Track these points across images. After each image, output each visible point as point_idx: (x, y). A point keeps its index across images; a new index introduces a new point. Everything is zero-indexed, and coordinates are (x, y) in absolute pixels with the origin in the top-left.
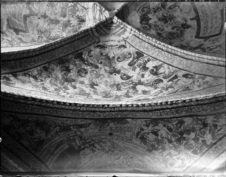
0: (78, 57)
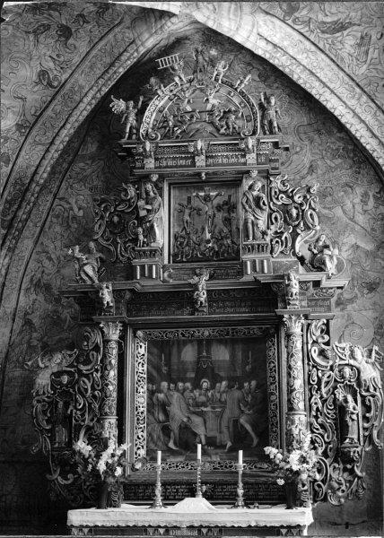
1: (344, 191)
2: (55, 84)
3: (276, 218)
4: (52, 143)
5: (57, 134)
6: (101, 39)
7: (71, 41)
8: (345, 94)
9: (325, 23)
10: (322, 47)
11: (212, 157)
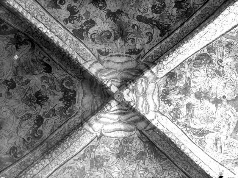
0: (167, 28)
2: (19, 156)
7: (41, 128)
9: (194, 129)
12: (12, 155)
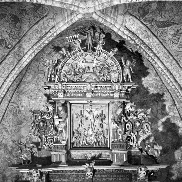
1: (154, 103)
2: (10, 46)
3: (128, 126)
4: (8, 77)
5: (11, 72)
6: (35, 24)
8: (164, 60)
9: (160, 22)
10: (156, 34)
11: (95, 93)
12: (4, 46)
